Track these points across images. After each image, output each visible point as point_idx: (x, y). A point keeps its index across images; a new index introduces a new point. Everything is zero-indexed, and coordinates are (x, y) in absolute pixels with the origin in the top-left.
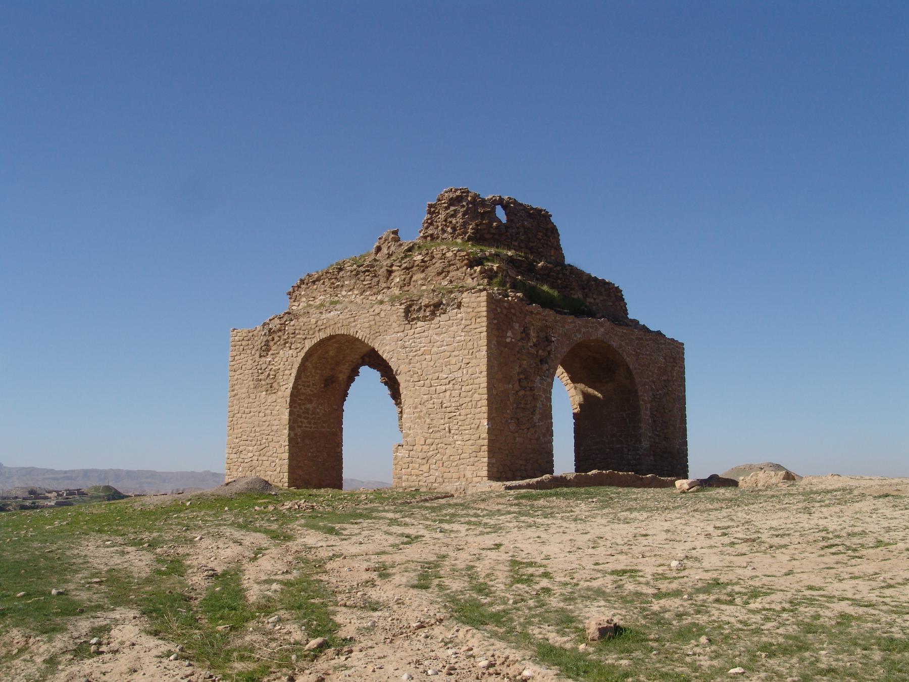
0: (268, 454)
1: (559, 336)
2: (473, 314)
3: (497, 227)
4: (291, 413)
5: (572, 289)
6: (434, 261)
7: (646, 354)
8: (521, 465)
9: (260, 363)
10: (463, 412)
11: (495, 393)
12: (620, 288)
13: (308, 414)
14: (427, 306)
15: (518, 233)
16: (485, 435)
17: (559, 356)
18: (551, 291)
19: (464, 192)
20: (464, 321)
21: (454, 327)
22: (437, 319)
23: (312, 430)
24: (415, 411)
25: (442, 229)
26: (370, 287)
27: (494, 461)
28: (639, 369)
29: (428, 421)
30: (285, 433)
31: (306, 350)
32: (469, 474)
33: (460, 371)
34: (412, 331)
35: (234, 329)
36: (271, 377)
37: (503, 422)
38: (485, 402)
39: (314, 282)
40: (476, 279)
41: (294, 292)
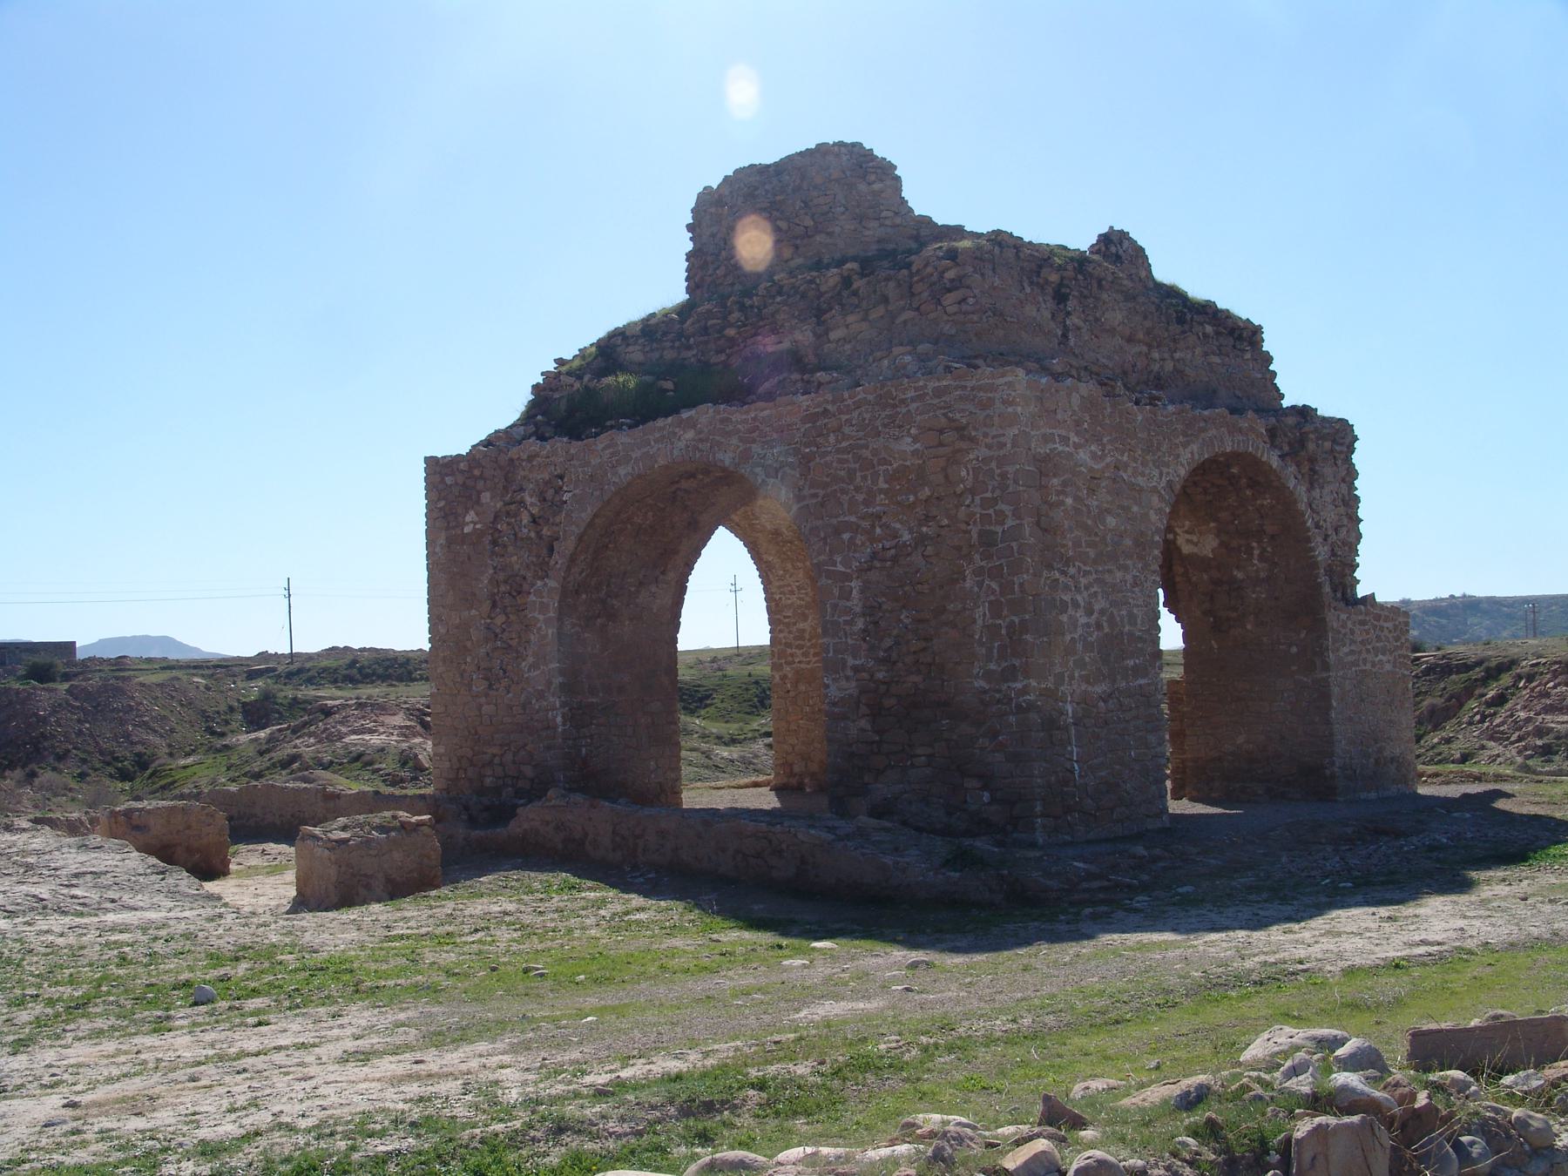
7: (839, 451)
8: (494, 756)
17: (573, 528)
28: (815, 496)
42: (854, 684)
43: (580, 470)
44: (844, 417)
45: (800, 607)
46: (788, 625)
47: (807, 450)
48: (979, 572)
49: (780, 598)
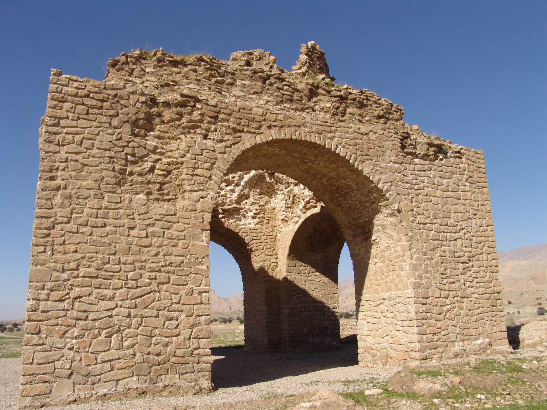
10: (476, 263)
20: (466, 172)
33: (469, 220)
39: (175, 64)
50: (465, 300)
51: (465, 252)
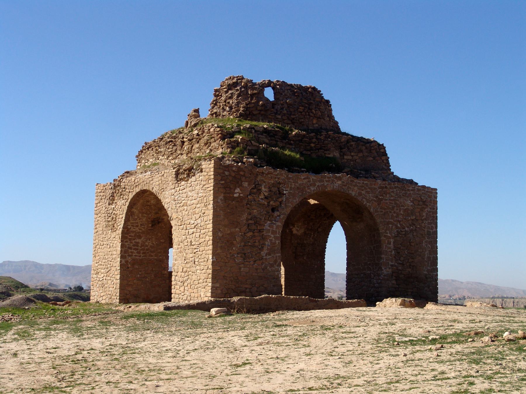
0: (111, 275)
1: (290, 190)
2: (207, 177)
3: (263, 105)
4: (122, 246)
5: (328, 150)
6: (204, 134)
7: (390, 200)
8: (246, 288)
9: (109, 209)
10: (201, 249)
11: (220, 234)
12: (384, 145)
13: (138, 246)
14: (185, 170)
15: (282, 109)
16: (210, 267)
17: (290, 205)
18: (293, 154)
19: (239, 79)
20: (202, 181)
21: (198, 186)
22: (190, 180)
23: (140, 258)
24: (179, 247)
25: (223, 108)
26: (172, 154)
27: (218, 285)
28: (382, 212)
29: (185, 254)
30: (118, 260)
31: (129, 200)
32: (202, 294)
34: (179, 188)
35: (98, 184)
36: (114, 219)
37: (229, 256)
38: (211, 242)
39: (148, 148)
40: (224, 148)
41: (139, 155)
42: (391, 270)
43: (293, 184)
44: (391, 190)
45: (139, 233)
46: (130, 239)
47: (380, 197)
48: (426, 242)
49: (130, 228)
50: (193, 273)
51: (196, 242)
